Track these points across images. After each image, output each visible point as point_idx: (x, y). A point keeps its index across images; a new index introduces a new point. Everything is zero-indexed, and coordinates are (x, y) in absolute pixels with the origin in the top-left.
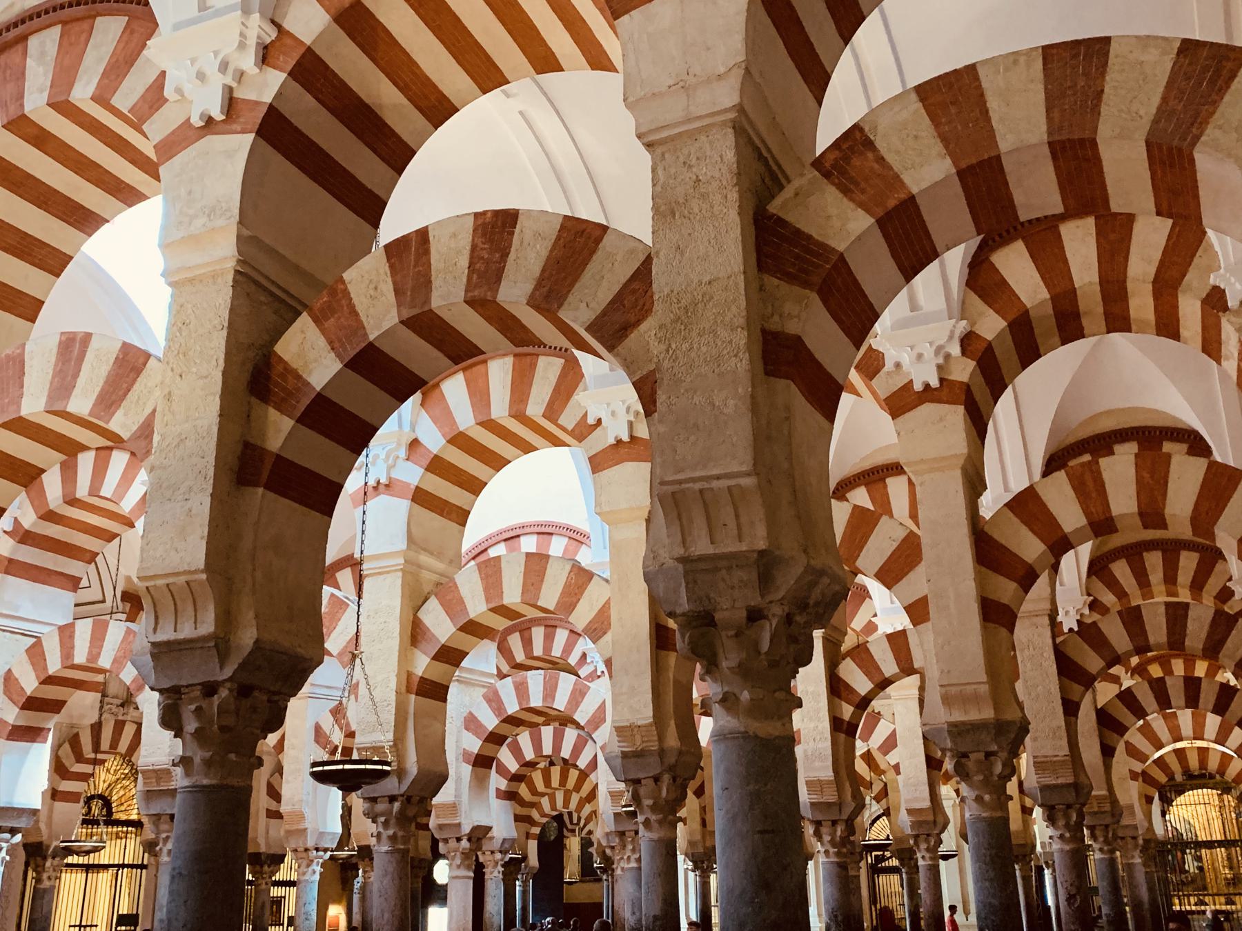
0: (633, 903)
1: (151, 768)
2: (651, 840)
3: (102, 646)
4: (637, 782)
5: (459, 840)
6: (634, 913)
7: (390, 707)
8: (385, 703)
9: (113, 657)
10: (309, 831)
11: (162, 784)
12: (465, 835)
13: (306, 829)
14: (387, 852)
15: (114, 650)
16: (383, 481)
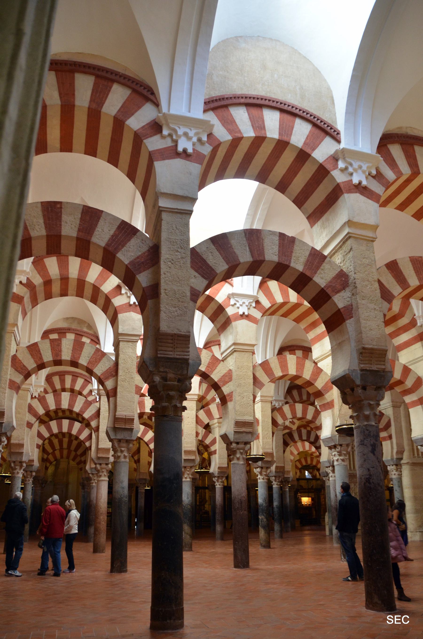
0: (188, 494)
1: (124, 417)
2: (344, 465)
3: (81, 354)
4: (341, 445)
5: (107, 464)
6: (188, 498)
7: (251, 407)
8: (249, 405)
9: (88, 361)
10: (24, 454)
11: (127, 425)
12: (111, 463)
13: (23, 453)
14: (242, 464)
15: (88, 357)
16: (246, 313)
